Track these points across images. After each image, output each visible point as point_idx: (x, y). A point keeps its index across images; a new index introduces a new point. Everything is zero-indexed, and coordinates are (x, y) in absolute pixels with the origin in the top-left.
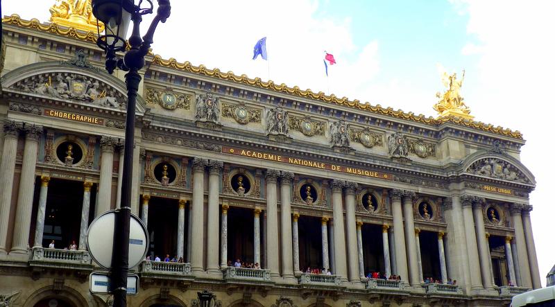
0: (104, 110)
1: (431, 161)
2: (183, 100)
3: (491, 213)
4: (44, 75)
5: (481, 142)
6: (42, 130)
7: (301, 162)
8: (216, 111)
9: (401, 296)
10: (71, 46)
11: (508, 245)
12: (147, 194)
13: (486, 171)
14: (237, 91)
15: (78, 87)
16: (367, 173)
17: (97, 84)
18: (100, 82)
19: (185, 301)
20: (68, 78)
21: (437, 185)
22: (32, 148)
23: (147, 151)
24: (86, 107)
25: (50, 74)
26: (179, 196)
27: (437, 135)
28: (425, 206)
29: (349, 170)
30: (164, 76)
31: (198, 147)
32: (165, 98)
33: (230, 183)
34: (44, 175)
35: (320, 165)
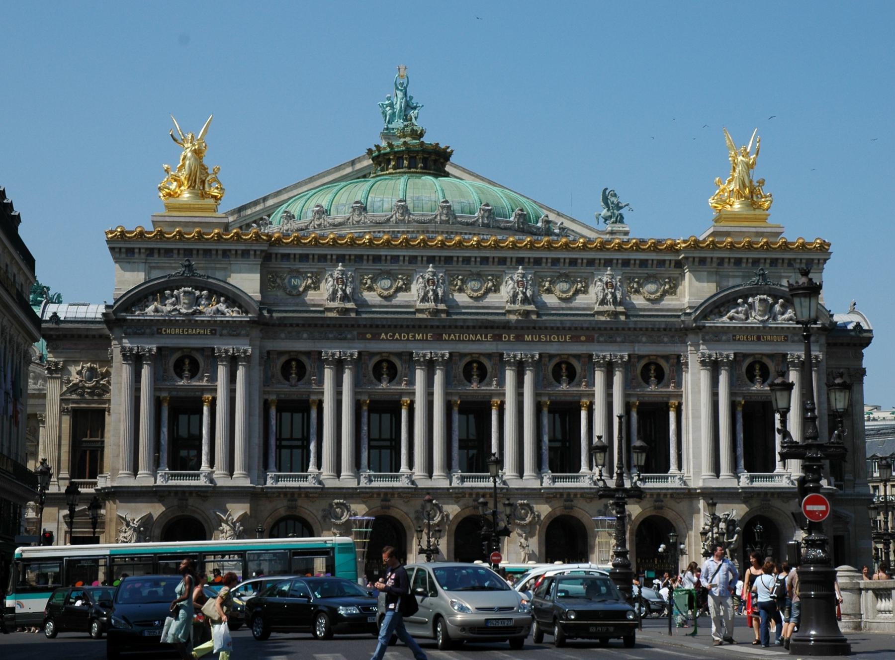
1: (669, 302)
3: (755, 370)
7: (459, 337)
10: (179, 250)
12: (273, 397)
14: (377, 259)
16: (554, 338)
17: (205, 292)
19: (314, 511)
21: (666, 339)
23: (268, 352)
26: (309, 396)
27: (679, 265)
28: (653, 367)
29: (528, 338)
30: (286, 257)
31: (328, 339)
32: (290, 282)
33: (371, 373)
34: (164, 394)
35: (486, 337)
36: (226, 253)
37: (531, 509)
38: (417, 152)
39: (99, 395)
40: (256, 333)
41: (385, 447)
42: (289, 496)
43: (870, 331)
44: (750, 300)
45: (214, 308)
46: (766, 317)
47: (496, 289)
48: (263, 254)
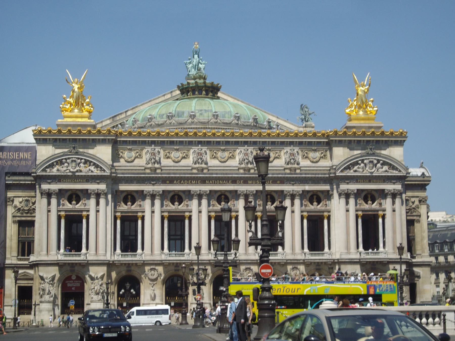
0: (88, 175)
2: (138, 154)
4: (56, 161)
5: (365, 143)
6: (58, 191)
7: (214, 182)
8: (157, 159)
9: (280, 262)
11: (380, 220)
13: (358, 169)
14: (172, 143)
15: (74, 164)
17: (83, 161)
18: (85, 159)
20: (68, 161)
21: (321, 182)
22: (54, 201)
23: (116, 191)
24: (78, 175)
25: (59, 160)
30: (125, 142)
36: (93, 140)
37: (252, 270)
38: (203, 87)
39: (31, 214)
40: (109, 181)
41: (178, 239)
42: (127, 265)
43: (429, 177)
44: (365, 161)
45: (88, 169)
46: (373, 170)
47: (232, 157)
48: (113, 141)
